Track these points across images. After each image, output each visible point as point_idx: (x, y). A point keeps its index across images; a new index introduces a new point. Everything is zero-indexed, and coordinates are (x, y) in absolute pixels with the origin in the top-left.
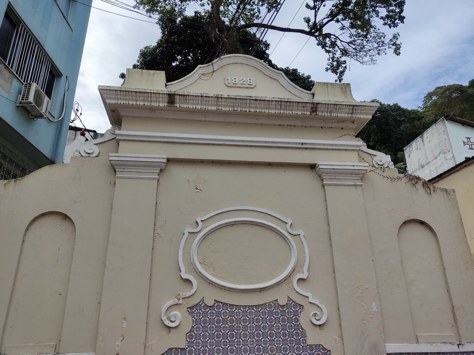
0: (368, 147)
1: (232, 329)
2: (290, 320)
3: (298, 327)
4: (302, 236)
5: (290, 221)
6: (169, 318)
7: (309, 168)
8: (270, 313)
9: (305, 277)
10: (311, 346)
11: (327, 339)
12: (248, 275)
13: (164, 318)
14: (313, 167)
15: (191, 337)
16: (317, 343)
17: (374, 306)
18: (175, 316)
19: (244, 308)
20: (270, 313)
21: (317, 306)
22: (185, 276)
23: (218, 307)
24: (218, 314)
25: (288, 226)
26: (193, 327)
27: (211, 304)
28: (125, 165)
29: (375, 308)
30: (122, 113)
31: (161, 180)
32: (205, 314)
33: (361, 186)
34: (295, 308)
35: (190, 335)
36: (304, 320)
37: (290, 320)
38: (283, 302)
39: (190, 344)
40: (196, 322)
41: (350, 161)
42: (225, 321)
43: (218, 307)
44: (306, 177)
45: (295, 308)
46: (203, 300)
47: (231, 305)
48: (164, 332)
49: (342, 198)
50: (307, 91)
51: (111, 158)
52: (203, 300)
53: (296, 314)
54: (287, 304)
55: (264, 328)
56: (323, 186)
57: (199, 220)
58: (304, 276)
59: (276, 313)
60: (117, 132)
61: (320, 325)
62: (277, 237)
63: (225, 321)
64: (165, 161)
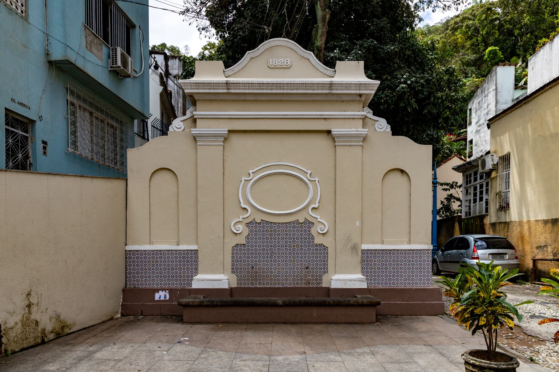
0: (374, 114)
1: (271, 235)
2: (305, 231)
3: (310, 234)
4: (317, 181)
5: (309, 172)
6: (236, 229)
7: (326, 135)
8: (294, 227)
10: (317, 244)
11: (326, 241)
12: (280, 207)
13: (233, 229)
14: (329, 132)
15: (248, 238)
16: (320, 243)
17: (358, 223)
18: (239, 228)
21: (322, 224)
22: (243, 206)
23: (263, 223)
24: (263, 227)
25: (308, 175)
27: (258, 221)
28: (202, 136)
29: (358, 224)
30: (196, 98)
31: (225, 146)
32: (256, 227)
33: (362, 146)
34: (309, 224)
35: (247, 237)
36: (313, 231)
37: (305, 231)
38: (301, 221)
39: (248, 242)
40: (251, 231)
41: (357, 129)
42: (267, 231)
43: (263, 223)
44: (322, 142)
45: (309, 224)
46: (254, 220)
48: (232, 235)
49: (348, 156)
50: (331, 69)
51: (192, 132)
52: (254, 220)
53: (309, 227)
55: (290, 235)
56: (335, 146)
57: (251, 172)
58: (316, 206)
60: (194, 113)
61: (323, 234)
62: (301, 182)
63: (267, 231)
64: (226, 132)
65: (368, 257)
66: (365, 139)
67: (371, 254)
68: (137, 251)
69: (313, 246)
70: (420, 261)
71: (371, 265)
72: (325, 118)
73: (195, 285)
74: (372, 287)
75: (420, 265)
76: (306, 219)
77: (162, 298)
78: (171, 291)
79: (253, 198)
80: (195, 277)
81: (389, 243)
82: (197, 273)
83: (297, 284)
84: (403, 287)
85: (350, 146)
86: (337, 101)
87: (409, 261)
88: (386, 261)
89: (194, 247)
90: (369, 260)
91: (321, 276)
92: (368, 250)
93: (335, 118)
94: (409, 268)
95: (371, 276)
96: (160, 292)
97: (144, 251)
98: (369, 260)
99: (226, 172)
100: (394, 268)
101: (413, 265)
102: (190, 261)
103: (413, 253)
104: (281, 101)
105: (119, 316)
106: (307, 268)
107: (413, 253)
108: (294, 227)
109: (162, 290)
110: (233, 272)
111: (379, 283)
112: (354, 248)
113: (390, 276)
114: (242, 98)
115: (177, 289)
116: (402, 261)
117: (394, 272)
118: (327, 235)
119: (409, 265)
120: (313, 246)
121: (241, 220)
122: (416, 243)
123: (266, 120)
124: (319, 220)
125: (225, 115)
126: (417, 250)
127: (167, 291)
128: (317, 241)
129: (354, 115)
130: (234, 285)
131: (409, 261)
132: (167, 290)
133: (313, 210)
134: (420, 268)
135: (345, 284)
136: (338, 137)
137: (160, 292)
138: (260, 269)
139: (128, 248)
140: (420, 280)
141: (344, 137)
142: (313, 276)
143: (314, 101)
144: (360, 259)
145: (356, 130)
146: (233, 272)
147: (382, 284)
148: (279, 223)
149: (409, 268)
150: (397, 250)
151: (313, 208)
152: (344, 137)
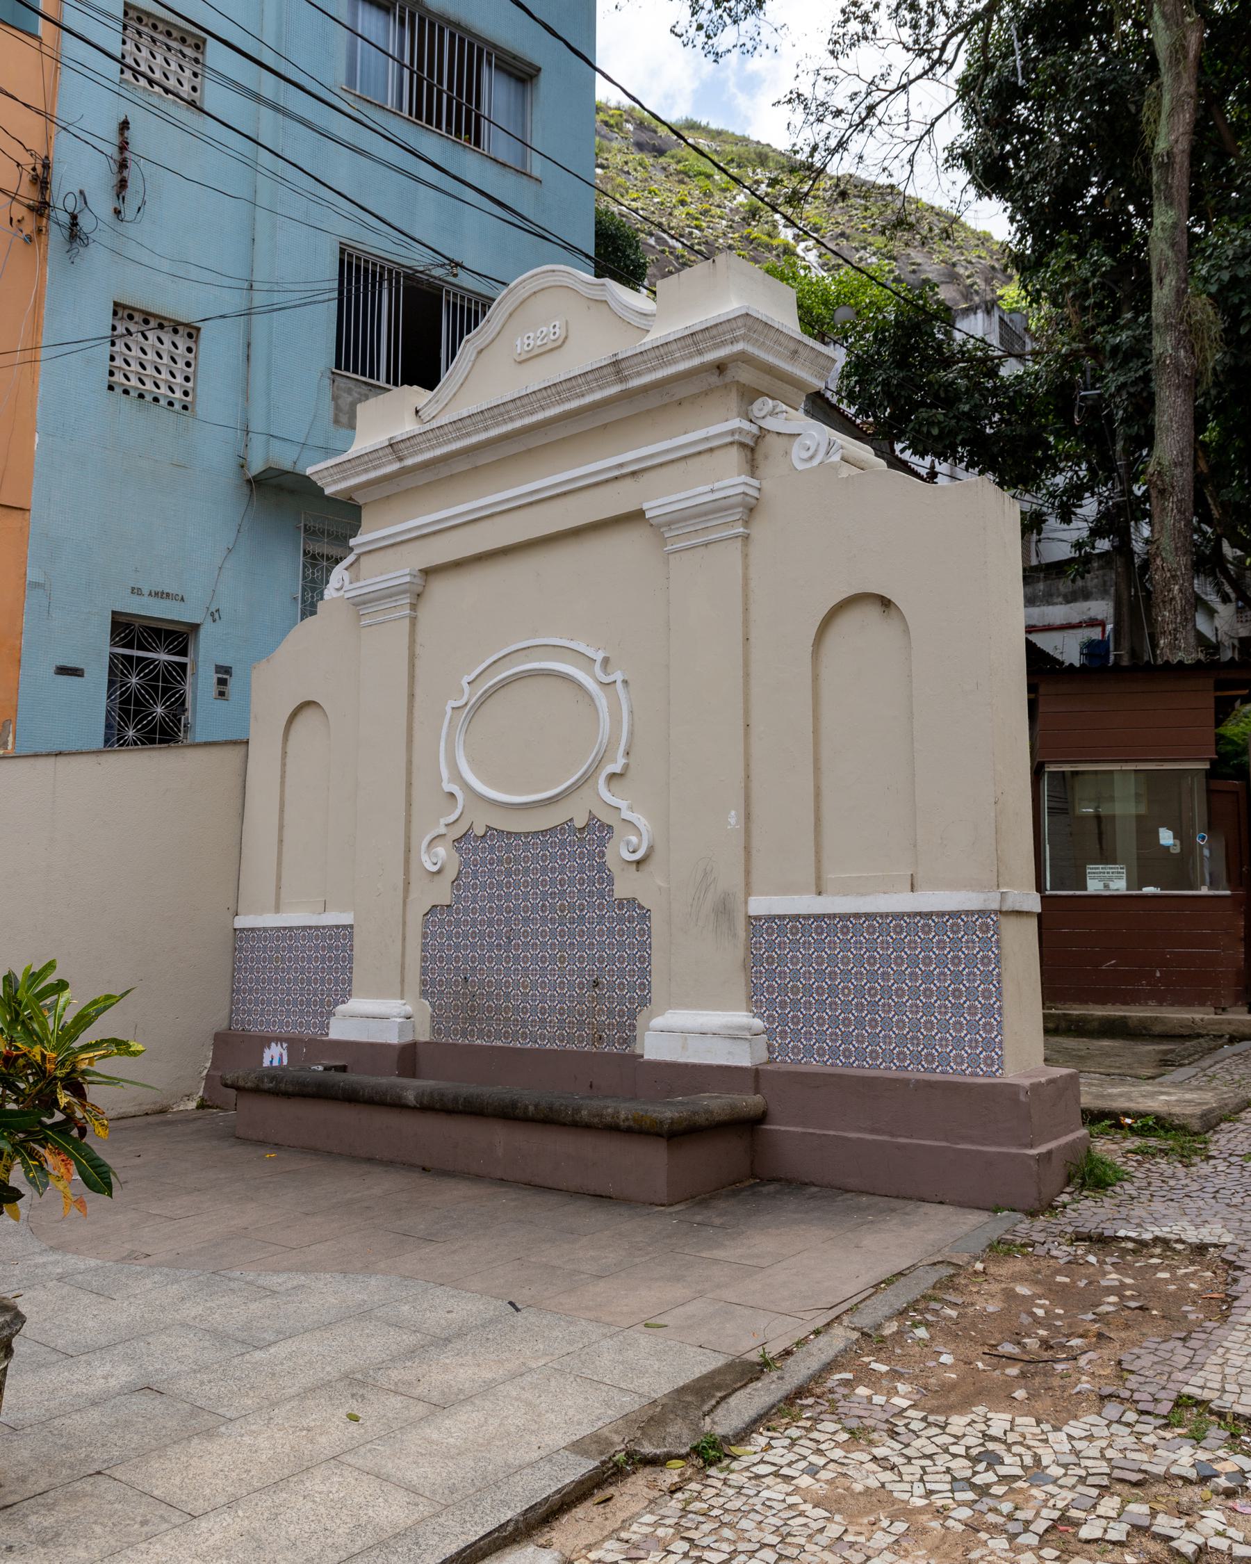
3: (602, 867)
4: (619, 685)
5: (599, 656)
9: (618, 771)
15: (458, 888)
19: (526, 838)
20: (563, 844)
26: (460, 872)
27: (481, 833)
29: (733, 821)
40: (465, 863)
47: (508, 833)
53: (602, 842)
54: (587, 825)
58: (616, 768)
59: (572, 844)
65: (771, 946)
66: (751, 509)
67: (781, 931)
68: (252, 930)
69: (610, 906)
70: (956, 961)
71: (782, 975)
72: (634, 473)
73: (340, 1030)
74: (788, 1062)
75: (957, 976)
76: (592, 817)
77: (276, 1063)
78: (293, 1044)
79: (472, 762)
80: (341, 1008)
81: (846, 889)
82: (346, 995)
83: (571, 1039)
84: (893, 1074)
85: (706, 545)
86: (665, 406)
87: (914, 962)
88: (832, 959)
89: (345, 918)
90: (777, 957)
91: (633, 1015)
92: (771, 918)
93: (661, 465)
94: (914, 992)
95: (783, 1020)
96: (273, 1045)
97: (265, 929)
98: (777, 957)
99: (419, 692)
100: (859, 991)
101: (928, 977)
102: (329, 958)
103: (926, 929)
104: (529, 451)
105: (192, 1105)
106: (596, 984)
107: (926, 929)
108: (563, 844)
109: (279, 1040)
110: (424, 994)
111: (808, 1050)
112: (724, 909)
113: (846, 1022)
114: (445, 471)
115: (301, 1040)
116: (886, 961)
117: (860, 1008)
118: (646, 868)
119: (913, 976)
120: (610, 906)
121: (442, 830)
122: (938, 884)
123: (497, 520)
124: (626, 814)
125: (410, 530)
126: (942, 914)
127: (285, 1045)
128: (621, 890)
129: (707, 439)
130: (423, 1035)
131: (914, 962)
132: (286, 1040)
133: (615, 783)
134: (957, 993)
135: (684, 1048)
136: (669, 524)
137: (273, 1045)
138: (482, 986)
139: (242, 922)
140: (958, 1043)
141: (685, 519)
142: (610, 1012)
143: (605, 426)
144: (740, 953)
145: (707, 488)
146: (424, 994)
147: (821, 1052)
148: (527, 834)
149: (914, 992)
150: (869, 916)
151: (612, 776)
152: (685, 519)
